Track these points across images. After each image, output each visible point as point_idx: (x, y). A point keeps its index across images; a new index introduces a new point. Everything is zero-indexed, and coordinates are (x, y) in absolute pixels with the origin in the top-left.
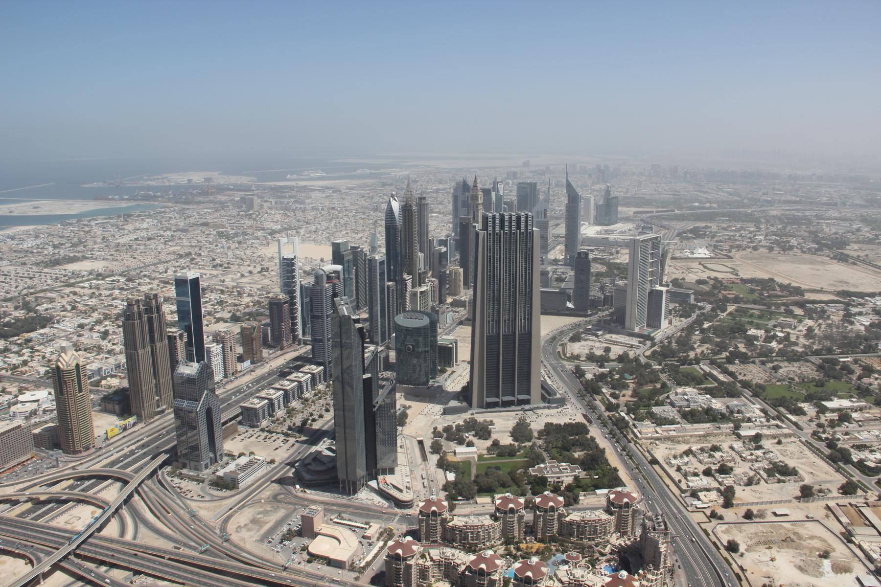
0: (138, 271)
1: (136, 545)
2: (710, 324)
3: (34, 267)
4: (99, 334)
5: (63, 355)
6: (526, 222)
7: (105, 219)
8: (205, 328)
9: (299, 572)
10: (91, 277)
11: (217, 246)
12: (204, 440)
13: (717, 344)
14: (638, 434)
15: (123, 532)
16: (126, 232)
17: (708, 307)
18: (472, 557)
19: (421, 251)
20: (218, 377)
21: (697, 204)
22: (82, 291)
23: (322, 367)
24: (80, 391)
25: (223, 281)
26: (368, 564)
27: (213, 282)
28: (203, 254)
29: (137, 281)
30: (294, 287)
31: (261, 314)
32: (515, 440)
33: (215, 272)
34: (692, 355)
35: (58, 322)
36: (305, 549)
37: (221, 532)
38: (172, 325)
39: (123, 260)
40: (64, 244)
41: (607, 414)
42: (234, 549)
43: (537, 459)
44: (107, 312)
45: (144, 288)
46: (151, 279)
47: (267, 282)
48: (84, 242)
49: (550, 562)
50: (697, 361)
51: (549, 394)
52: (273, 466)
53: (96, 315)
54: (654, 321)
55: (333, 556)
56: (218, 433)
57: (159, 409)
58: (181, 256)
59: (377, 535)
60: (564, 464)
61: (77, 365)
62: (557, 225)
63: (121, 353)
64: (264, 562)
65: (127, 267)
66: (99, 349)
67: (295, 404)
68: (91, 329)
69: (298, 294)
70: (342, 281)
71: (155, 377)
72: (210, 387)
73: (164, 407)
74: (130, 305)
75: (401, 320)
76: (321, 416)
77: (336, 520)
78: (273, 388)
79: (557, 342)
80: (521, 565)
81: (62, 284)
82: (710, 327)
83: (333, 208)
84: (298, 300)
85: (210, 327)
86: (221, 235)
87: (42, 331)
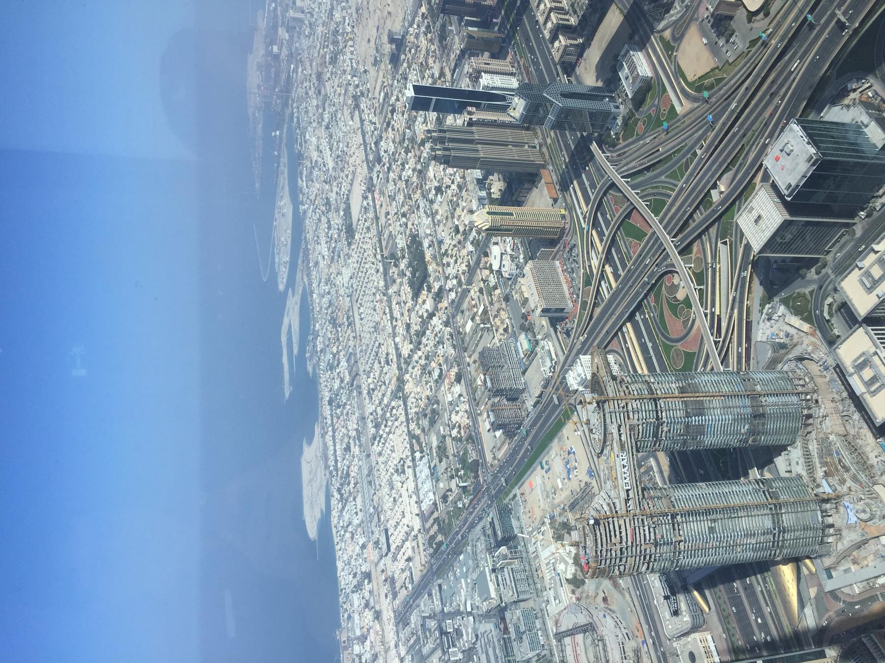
3: (352, 247)
4: (439, 196)
5: (476, 224)
7: (301, 179)
24: (512, 214)
29: (382, 153)
31: (443, 26)
36: (751, 15)
46: (381, 140)
57: (538, 147)
58: (357, 106)
61: (488, 213)
64: (751, 61)
65: (363, 162)
71: (507, 145)
73: (536, 142)
74: (435, 158)
86: (334, 60)
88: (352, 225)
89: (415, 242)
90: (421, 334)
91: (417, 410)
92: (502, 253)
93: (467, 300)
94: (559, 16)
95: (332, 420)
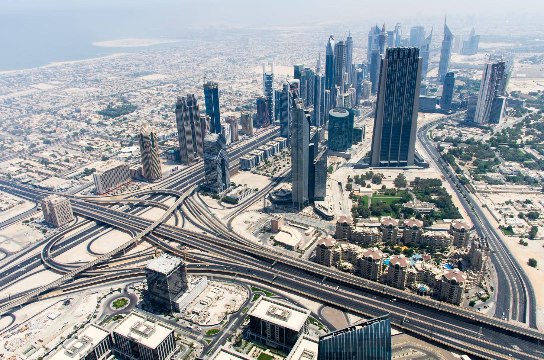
0: (183, 81)
1: (183, 230)
2: (535, 122)
6: (415, 53)
8: (221, 115)
9: (269, 250)
10: (157, 84)
11: (227, 66)
12: (220, 176)
13: (538, 136)
14: (475, 188)
15: (177, 224)
16: (176, 57)
17: (535, 111)
18: (365, 250)
19: (347, 71)
20: (228, 142)
21: (537, 40)
22: (153, 92)
23: (286, 139)
24: (154, 147)
25: (231, 88)
26: (307, 249)
27: (225, 88)
28: (219, 71)
30: (271, 91)
31: (253, 107)
32: (397, 186)
33: (226, 82)
34: (519, 142)
35: (141, 109)
36: (272, 238)
37: (228, 226)
38: (203, 112)
39: (174, 74)
40: (142, 64)
41: (456, 174)
42: (235, 235)
43: (408, 198)
44: (167, 104)
45: (187, 91)
47: (256, 88)
48: (152, 63)
49: (411, 258)
50: (522, 146)
51: (420, 160)
52: (257, 192)
53: (161, 106)
54: (493, 118)
55: (288, 243)
56: (227, 173)
57: (195, 159)
59: (313, 233)
60: (424, 202)
61: (152, 133)
62: (435, 55)
63: (175, 127)
66: (163, 125)
67: (270, 159)
68: (159, 114)
69: (273, 96)
70: (299, 89)
71: (194, 142)
72: (224, 148)
73: (199, 157)
74: (179, 101)
75: (332, 113)
76: (284, 166)
77: (290, 224)
78: (258, 149)
79: (428, 129)
80: (394, 258)
81: (142, 87)
82: (534, 124)
83: (295, 44)
84: (273, 99)
85: (224, 114)
86: (229, 60)
87: (132, 114)
88: (140, 76)
89: (133, 108)
90: (74, 118)
91: (21, 122)
92: (131, 152)
93: (100, 139)
94: (263, 156)
95: (6, 77)
